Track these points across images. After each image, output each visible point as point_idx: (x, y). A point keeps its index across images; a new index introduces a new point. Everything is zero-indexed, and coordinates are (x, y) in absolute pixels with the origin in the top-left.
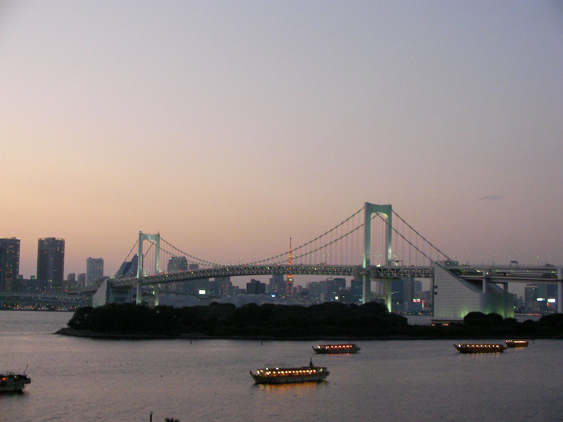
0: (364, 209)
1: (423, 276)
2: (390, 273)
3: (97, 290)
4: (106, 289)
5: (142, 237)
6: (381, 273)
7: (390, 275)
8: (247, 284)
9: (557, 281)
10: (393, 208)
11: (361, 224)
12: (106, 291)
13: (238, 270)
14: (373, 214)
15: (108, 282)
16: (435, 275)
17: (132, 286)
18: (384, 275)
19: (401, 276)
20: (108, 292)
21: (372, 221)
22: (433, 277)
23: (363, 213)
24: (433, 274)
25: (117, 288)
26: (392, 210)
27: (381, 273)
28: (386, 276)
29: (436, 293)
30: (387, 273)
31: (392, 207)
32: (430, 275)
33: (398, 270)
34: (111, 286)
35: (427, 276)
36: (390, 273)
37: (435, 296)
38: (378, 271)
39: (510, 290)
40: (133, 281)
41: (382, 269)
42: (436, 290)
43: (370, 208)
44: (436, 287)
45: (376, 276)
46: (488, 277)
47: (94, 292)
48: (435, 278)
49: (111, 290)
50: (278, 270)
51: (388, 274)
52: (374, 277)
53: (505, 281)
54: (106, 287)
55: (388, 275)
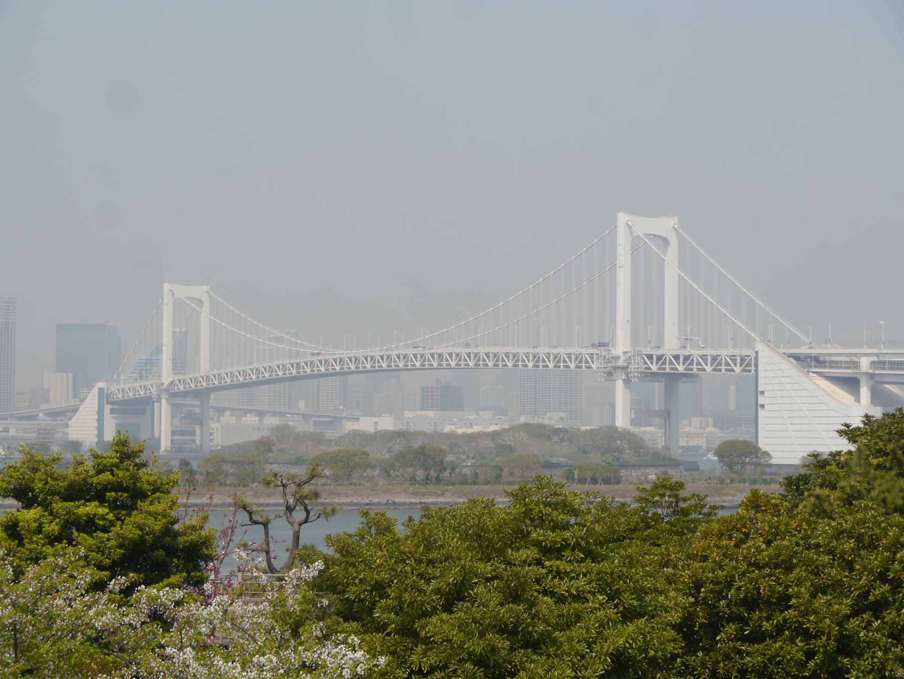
1: (738, 369)
2: (671, 363)
3: (79, 408)
4: (96, 405)
6: (652, 363)
8: (423, 388)
12: (97, 410)
13: (366, 360)
15: (101, 390)
17: (150, 397)
18: (659, 369)
19: (692, 370)
20: (100, 413)
22: (756, 371)
25: (119, 403)
28: (663, 371)
29: (763, 406)
30: (664, 363)
32: (753, 368)
33: (686, 358)
34: (107, 399)
36: (671, 363)
37: (761, 413)
40: (154, 387)
41: (655, 358)
44: (763, 393)
45: (643, 370)
46: (871, 371)
47: (75, 410)
48: (761, 374)
49: (107, 408)
51: (667, 366)
52: (638, 372)
54: (97, 401)
55: (665, 369)
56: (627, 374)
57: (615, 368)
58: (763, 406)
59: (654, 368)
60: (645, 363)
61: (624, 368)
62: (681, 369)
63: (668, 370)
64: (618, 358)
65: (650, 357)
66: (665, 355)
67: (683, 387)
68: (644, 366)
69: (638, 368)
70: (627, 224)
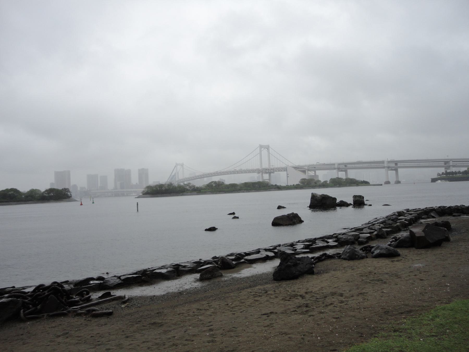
0: (259, 148)
9: (335, 169)
10: (270, 146)
14: (263, 149)
16: (288, 170)
22: (287, 171)
24: (287, 169)
29: (288, 177)
33: (273, 169)
35: (284, 171)
37: (288, 178)
38: (266, 170)
39: (317, 174)
42: (288, 176)
43: (261, 147)
44: (288, 174)
48: (288, 171)
53: (315, 170)
56: (262, 173)
57: (260, 172)
58: (288, 177)
59: (267, 171)
60: (265, 171)
61: (261, 172)
62: (272, 171)
64: (261, 170)
65: (266, 169)
67: (272, 174)
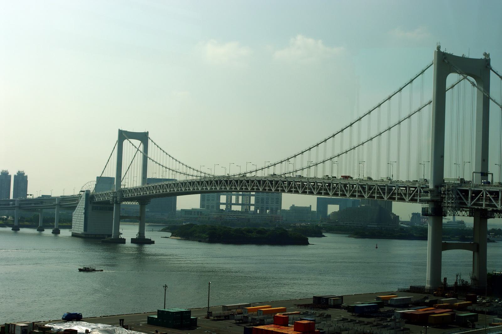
5: (123, 135)
7: (487, 205)
11: (426, 101)
18: (474, 204)
21: (448, 94)
23: (431, 75)
26: (491, 69)
27: (467, 199)
28: (480, 208)
31: (491, 64)
34: (90, 201)
49: (90, 207)
50: (269, 186)
51: (484, 203)
52: (452, 207)
55: (482, 205)
60: (460, 198)
63: (484, 207)
66: (482, 191)
68: (459, 201)
69: (452, 203)
70: (444, 61)
